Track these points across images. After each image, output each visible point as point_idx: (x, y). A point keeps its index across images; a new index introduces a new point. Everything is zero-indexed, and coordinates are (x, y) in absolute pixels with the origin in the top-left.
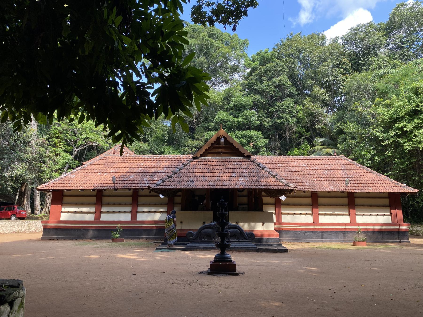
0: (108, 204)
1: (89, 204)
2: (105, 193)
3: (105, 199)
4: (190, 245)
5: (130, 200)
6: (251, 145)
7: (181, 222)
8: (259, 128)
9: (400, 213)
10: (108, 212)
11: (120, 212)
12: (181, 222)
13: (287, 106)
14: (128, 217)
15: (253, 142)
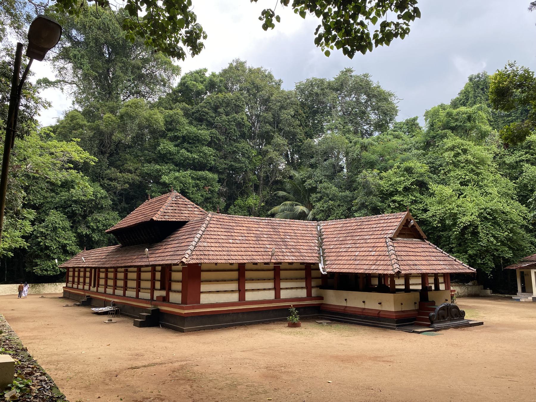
0: (252, 280)
1: (232, 281)
2: (247, 267)
3: (248, 274)
4: (436, 325)
5: (271, 274)
6: (207, 189)
7: (402, 304)
8: (212, 169)
9: (482, 286)
10: (253, 290)
11: (264, 289)
12: (402, 304)
13: (247, 150)
14: (270, 295)
15: (209, 186)
